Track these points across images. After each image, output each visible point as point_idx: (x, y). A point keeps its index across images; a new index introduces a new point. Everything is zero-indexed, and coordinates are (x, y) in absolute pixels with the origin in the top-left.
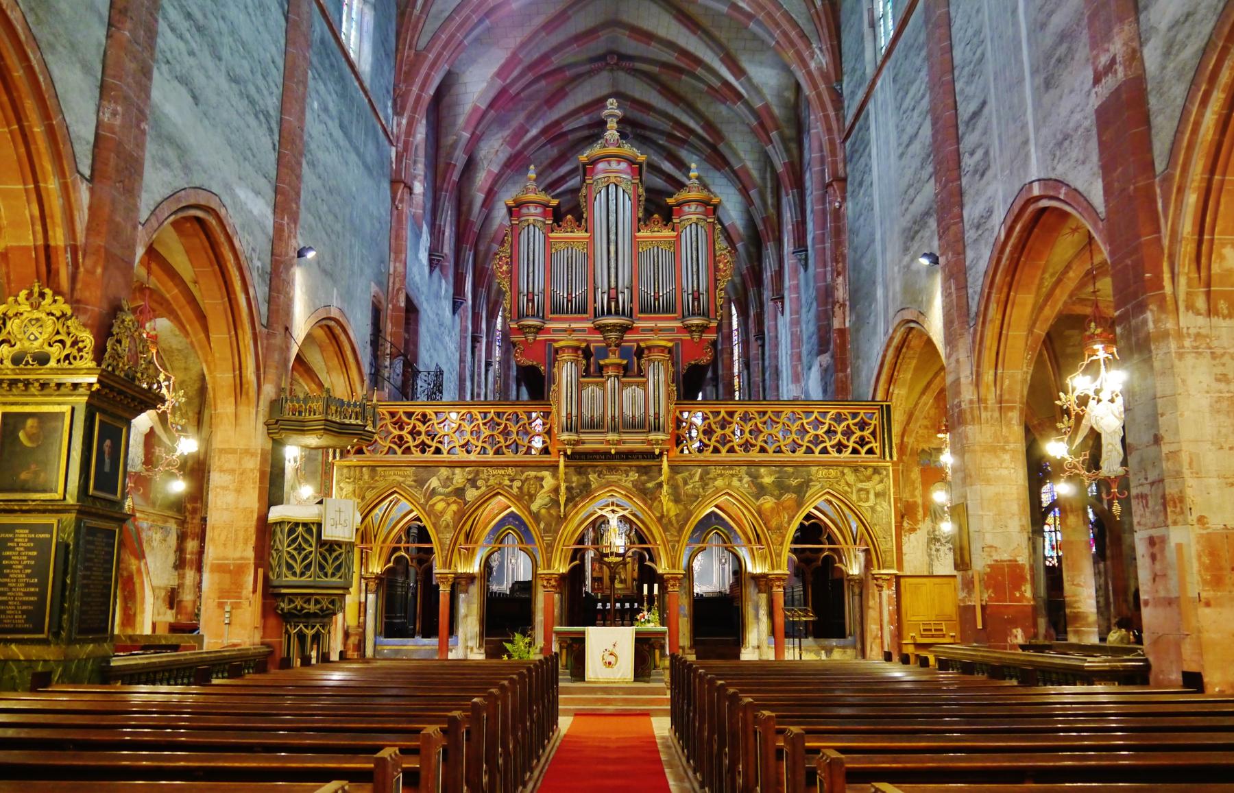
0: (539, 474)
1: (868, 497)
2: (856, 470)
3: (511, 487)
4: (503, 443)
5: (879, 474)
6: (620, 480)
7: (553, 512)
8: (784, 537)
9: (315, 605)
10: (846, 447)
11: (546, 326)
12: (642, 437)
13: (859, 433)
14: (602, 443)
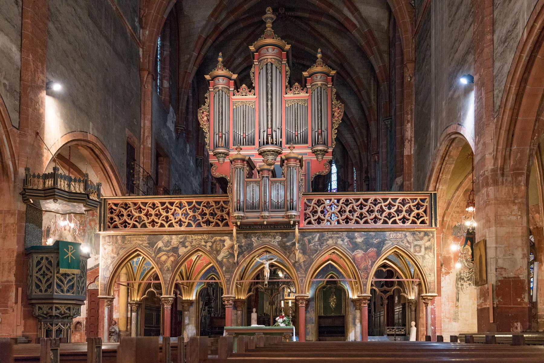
0: (222, 238)
1: (420, 250)
2: (413, 233)
3: (205, 246)
4: (201, 221)
5: (428, 236)
6: (271, 241)
7: (231, 260)
8: (368, 274)
9: (56, 310)
10: (408, 220)
11: (230, 153)
12: (283, 214)
13: (416, 211)
14: (259, 218)
